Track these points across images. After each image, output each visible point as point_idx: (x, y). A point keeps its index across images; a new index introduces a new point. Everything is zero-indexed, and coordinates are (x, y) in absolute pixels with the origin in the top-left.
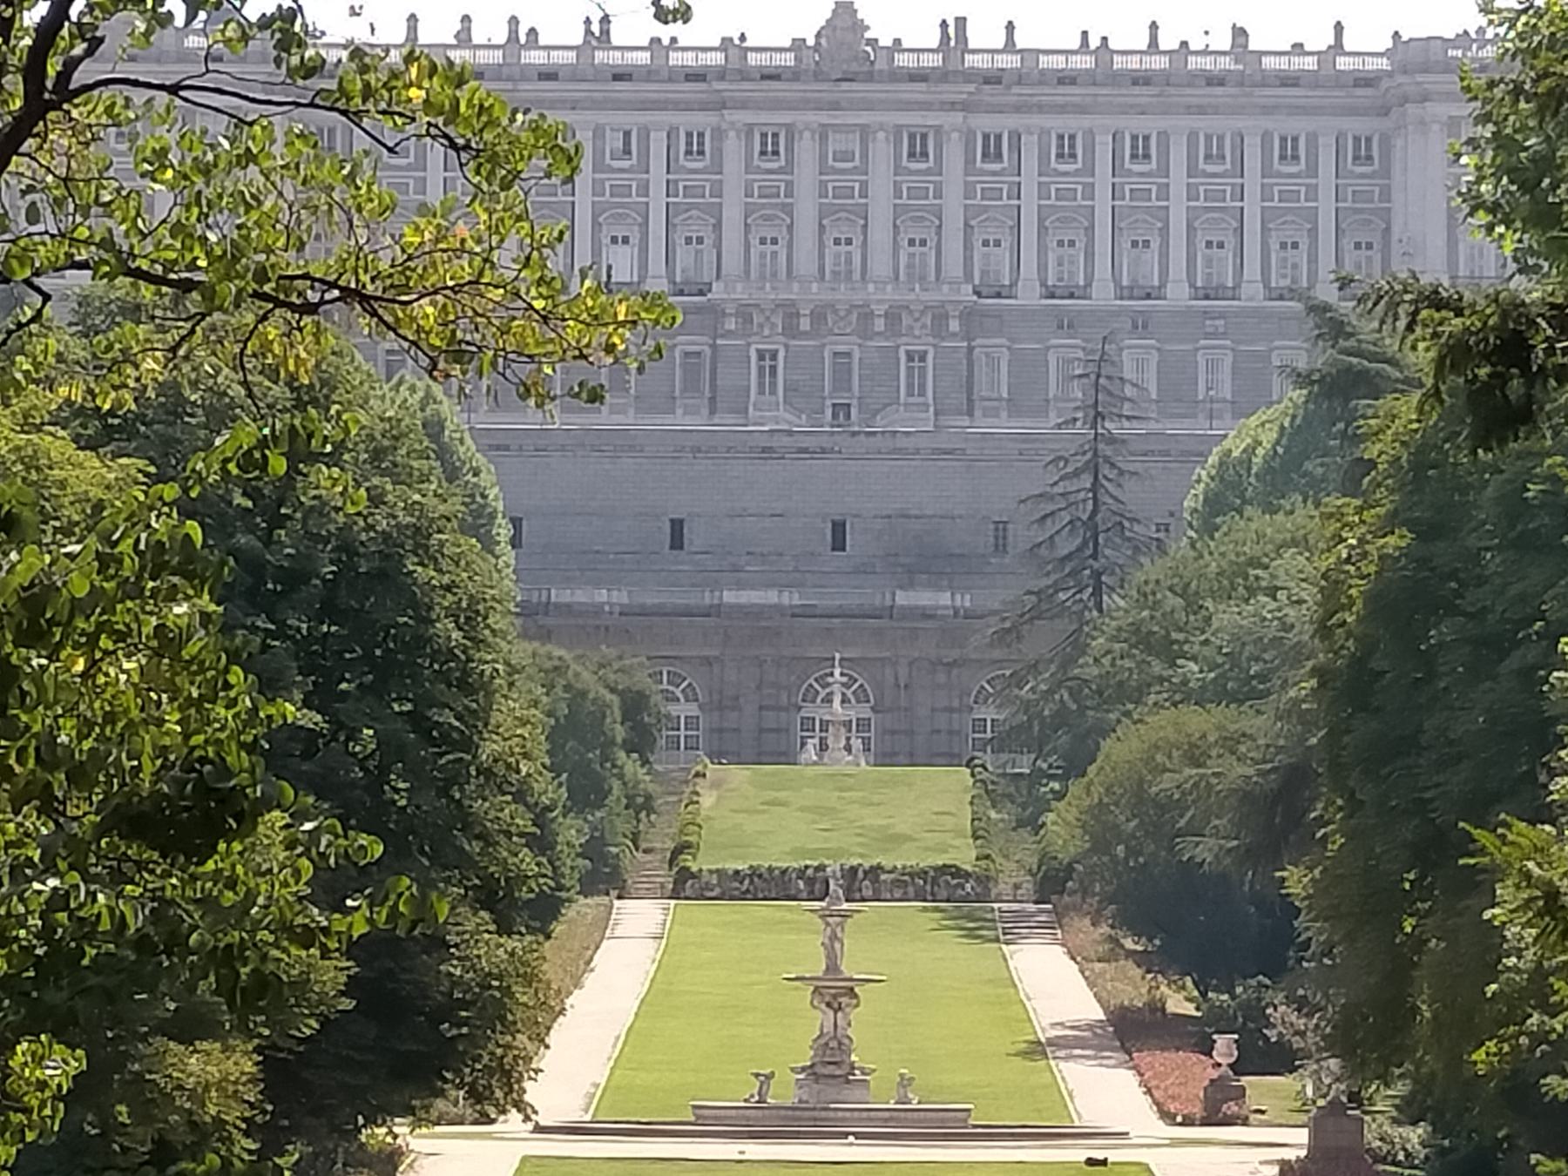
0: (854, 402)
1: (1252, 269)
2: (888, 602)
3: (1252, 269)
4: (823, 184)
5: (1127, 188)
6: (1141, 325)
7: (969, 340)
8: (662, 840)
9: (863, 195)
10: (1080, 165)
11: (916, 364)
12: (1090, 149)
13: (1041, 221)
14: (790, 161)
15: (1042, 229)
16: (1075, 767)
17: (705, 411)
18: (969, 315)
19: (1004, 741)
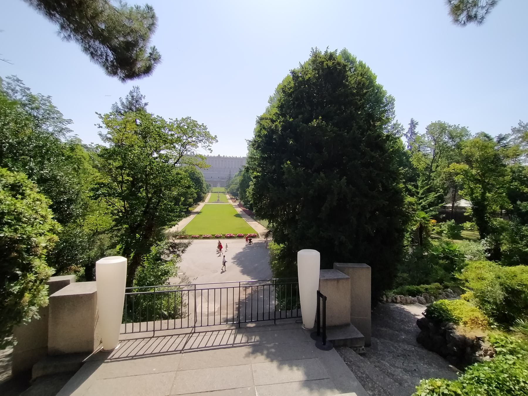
8: (211, 190)
16: (229, 187)
19: (226, 187)
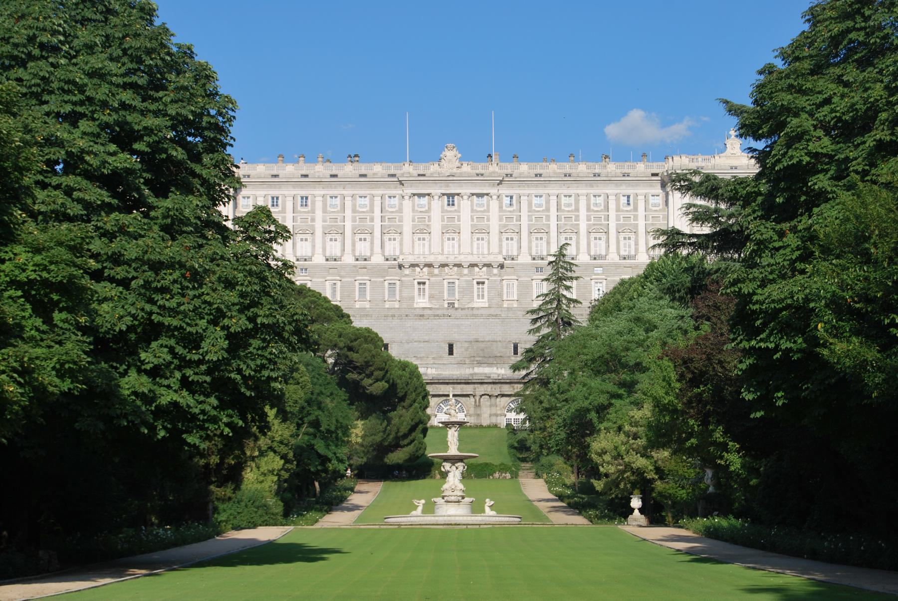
0: (456, 302)
1: (613, 248)
3: (613, 248)
4: (443, 217)
5: (563, 217)
9: (459, 220)
14: (429, 208)
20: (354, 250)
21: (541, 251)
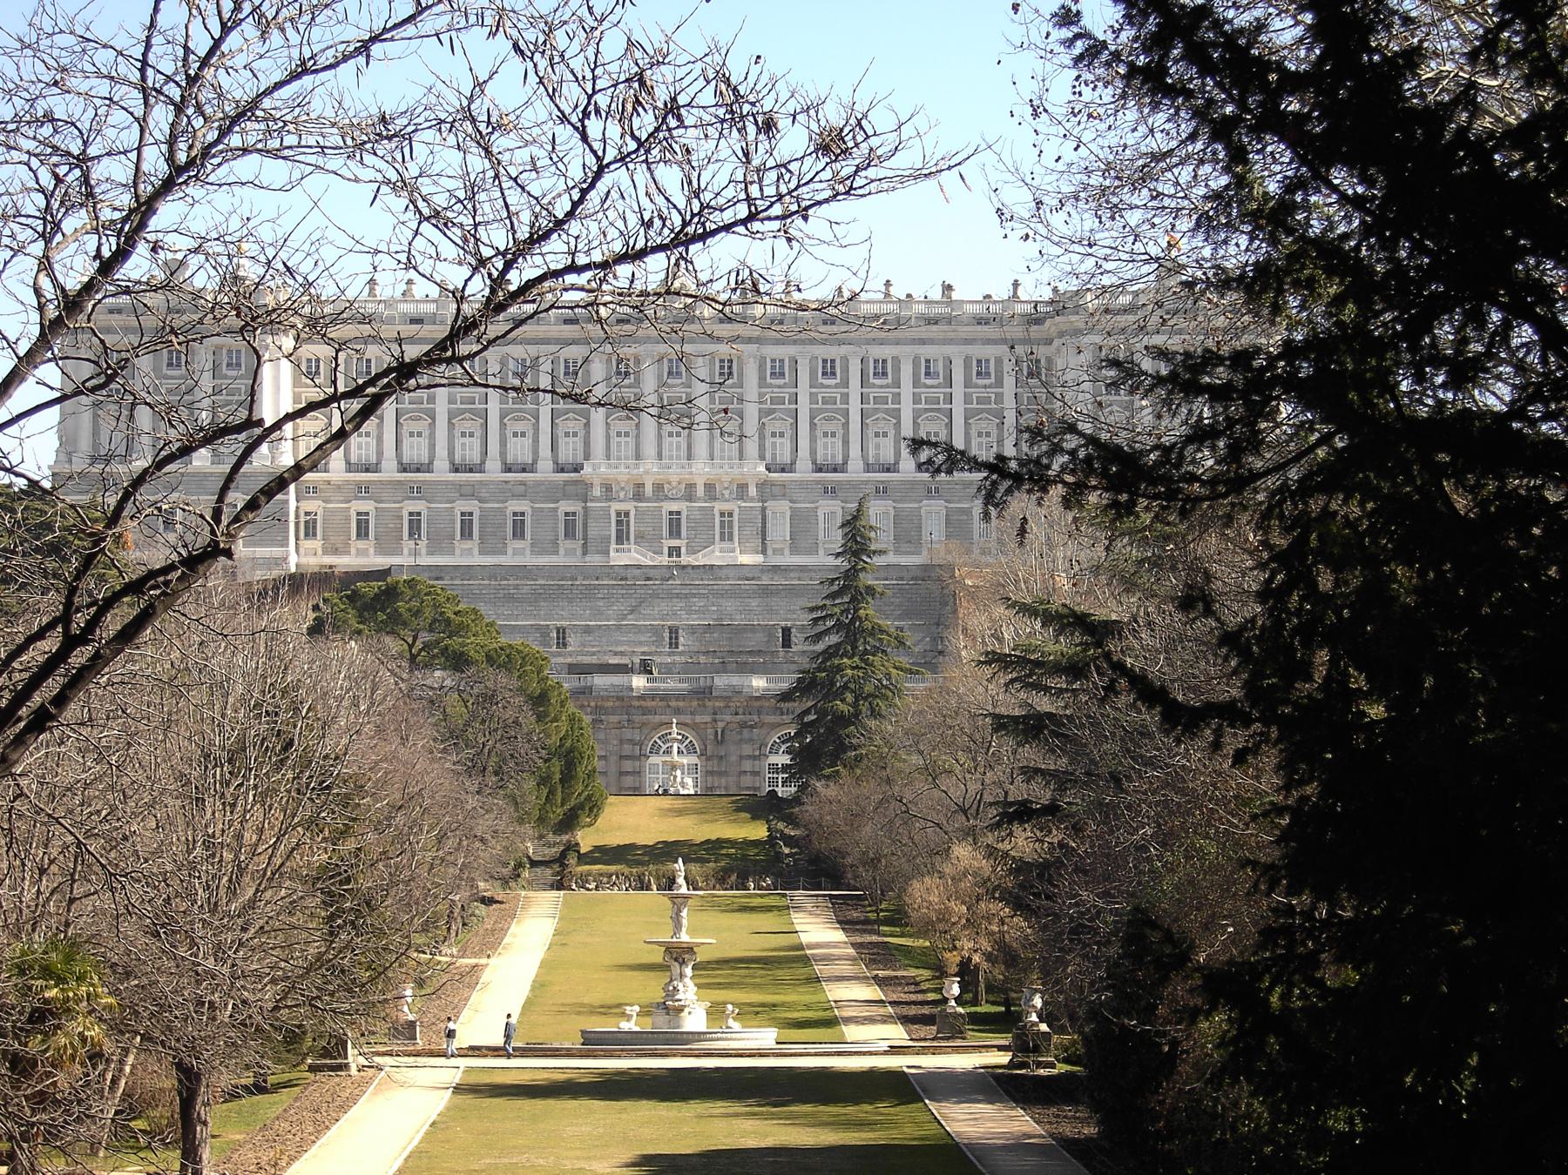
2: (709, 683)
6: (882, 491)
7: (764, 501)
10: (838, 381)
11: (726, 519)
12: (846, 370)
13: (812, 418)
15: (813, 426)
17: (579, 552)
18: (762, 485)
20: (503, 454)
21: (833, 456)
